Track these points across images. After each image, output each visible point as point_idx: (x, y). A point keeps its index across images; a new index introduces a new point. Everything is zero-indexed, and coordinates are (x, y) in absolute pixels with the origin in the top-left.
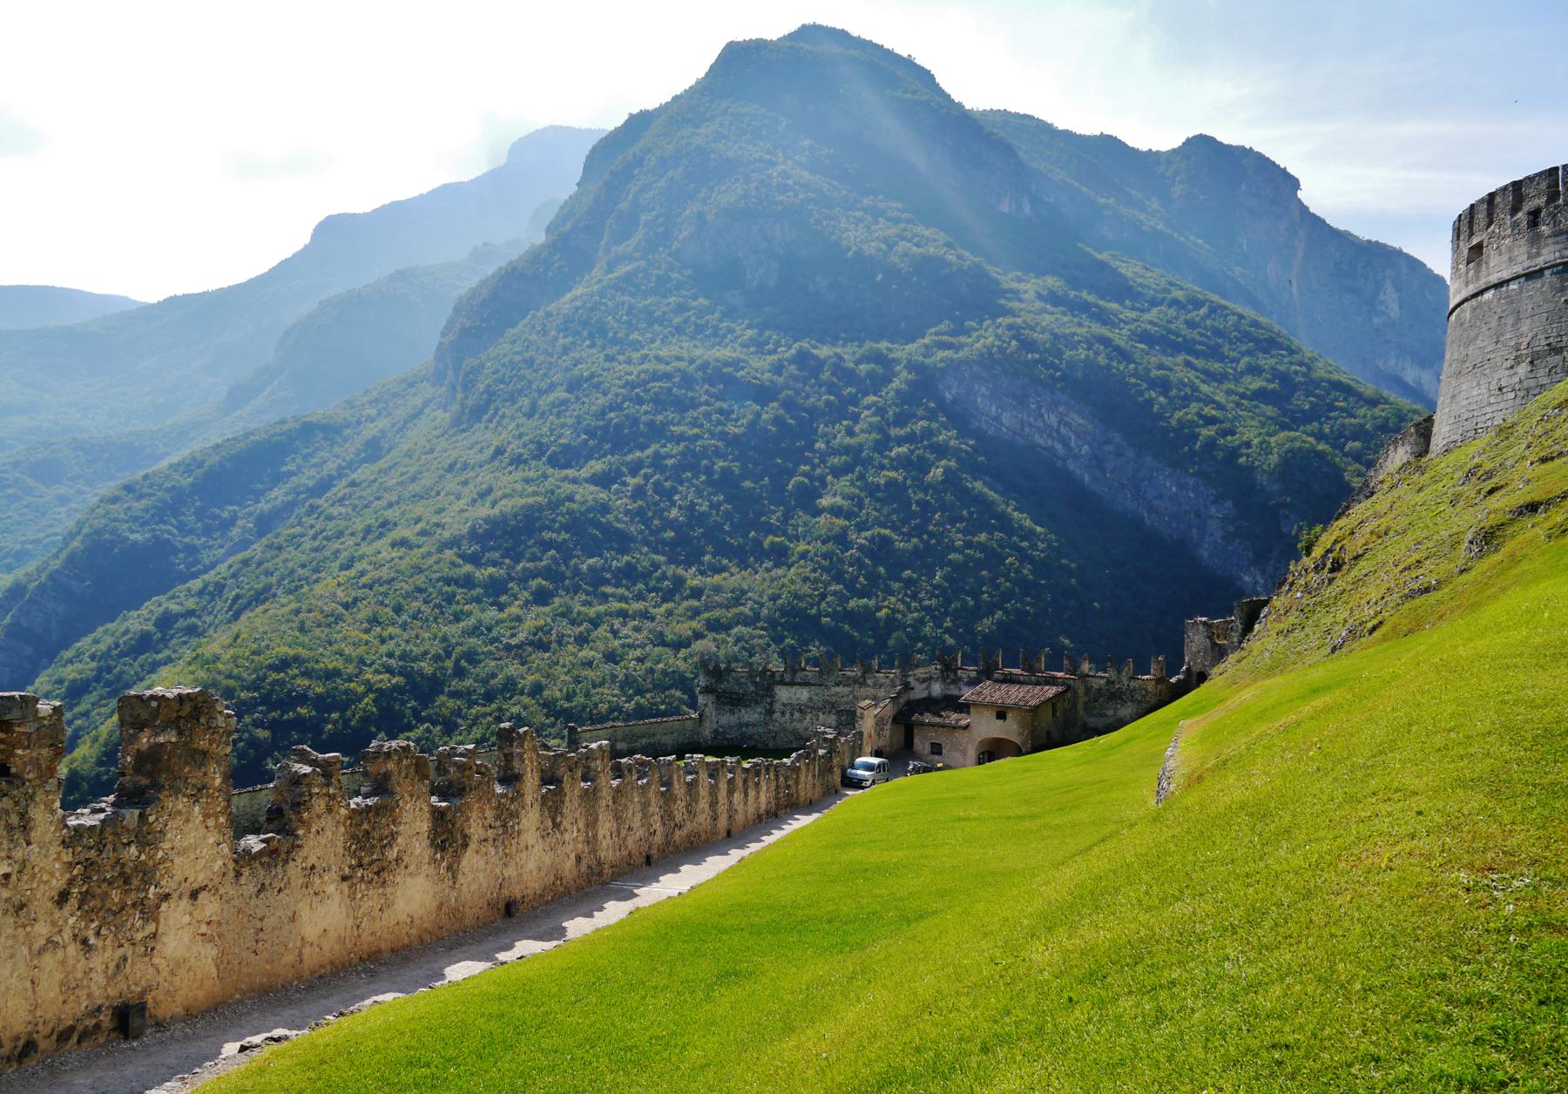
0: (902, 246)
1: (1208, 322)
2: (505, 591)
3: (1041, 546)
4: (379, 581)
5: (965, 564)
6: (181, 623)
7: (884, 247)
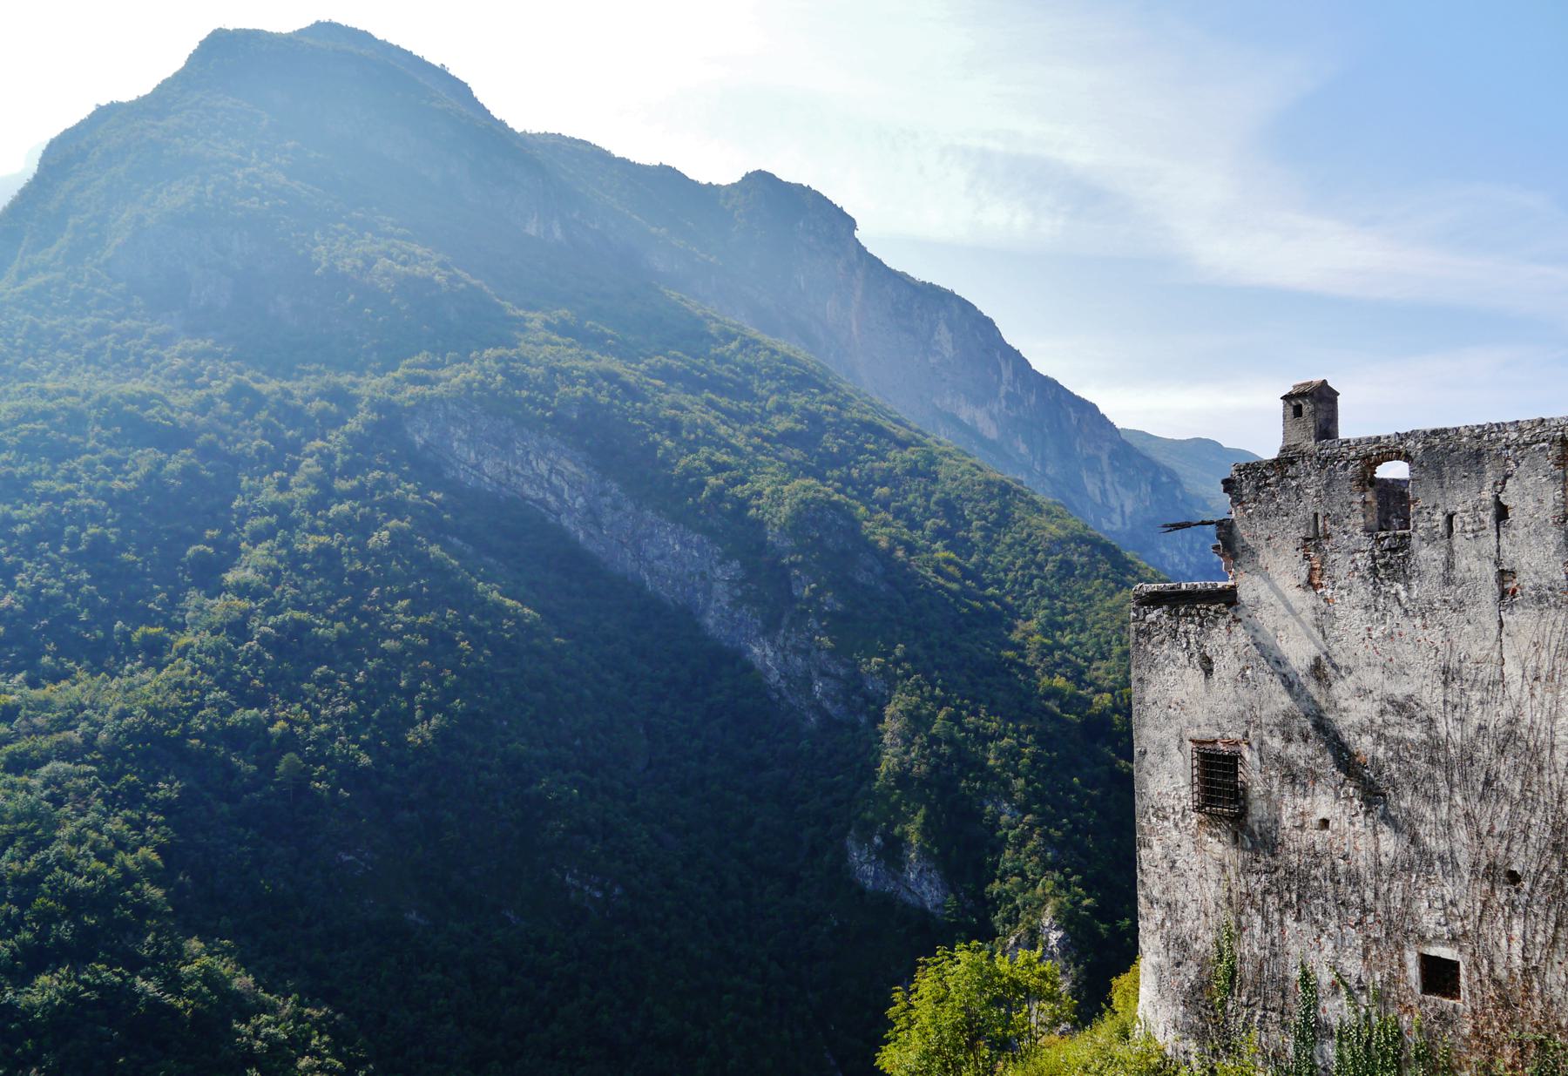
0: (383, 263)
1: (739, 357)
3: (507, 624)
5: (404, 652)
7: (359, 263)
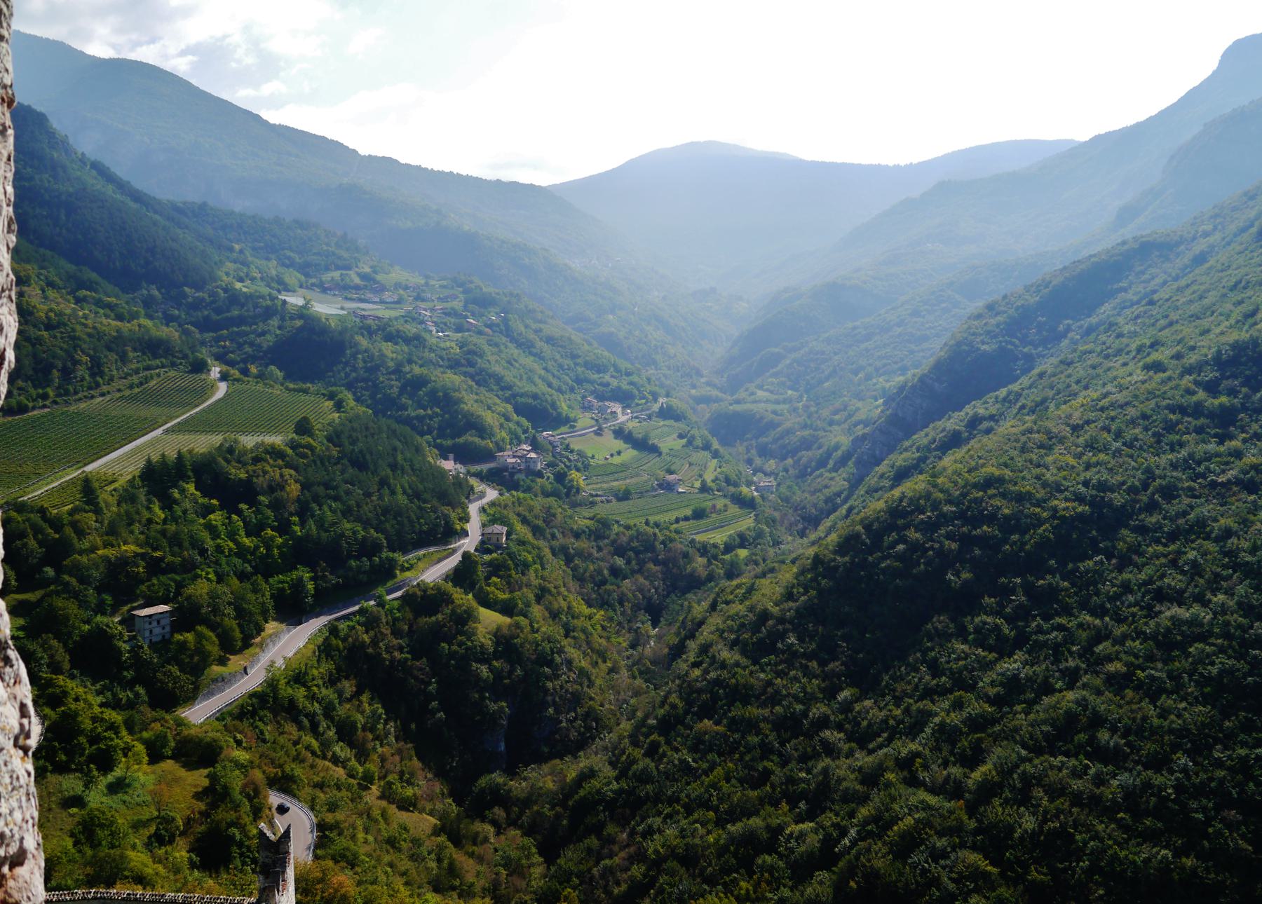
2: (1233, 422)
4: (1113, 405)
6: (985, 425)
